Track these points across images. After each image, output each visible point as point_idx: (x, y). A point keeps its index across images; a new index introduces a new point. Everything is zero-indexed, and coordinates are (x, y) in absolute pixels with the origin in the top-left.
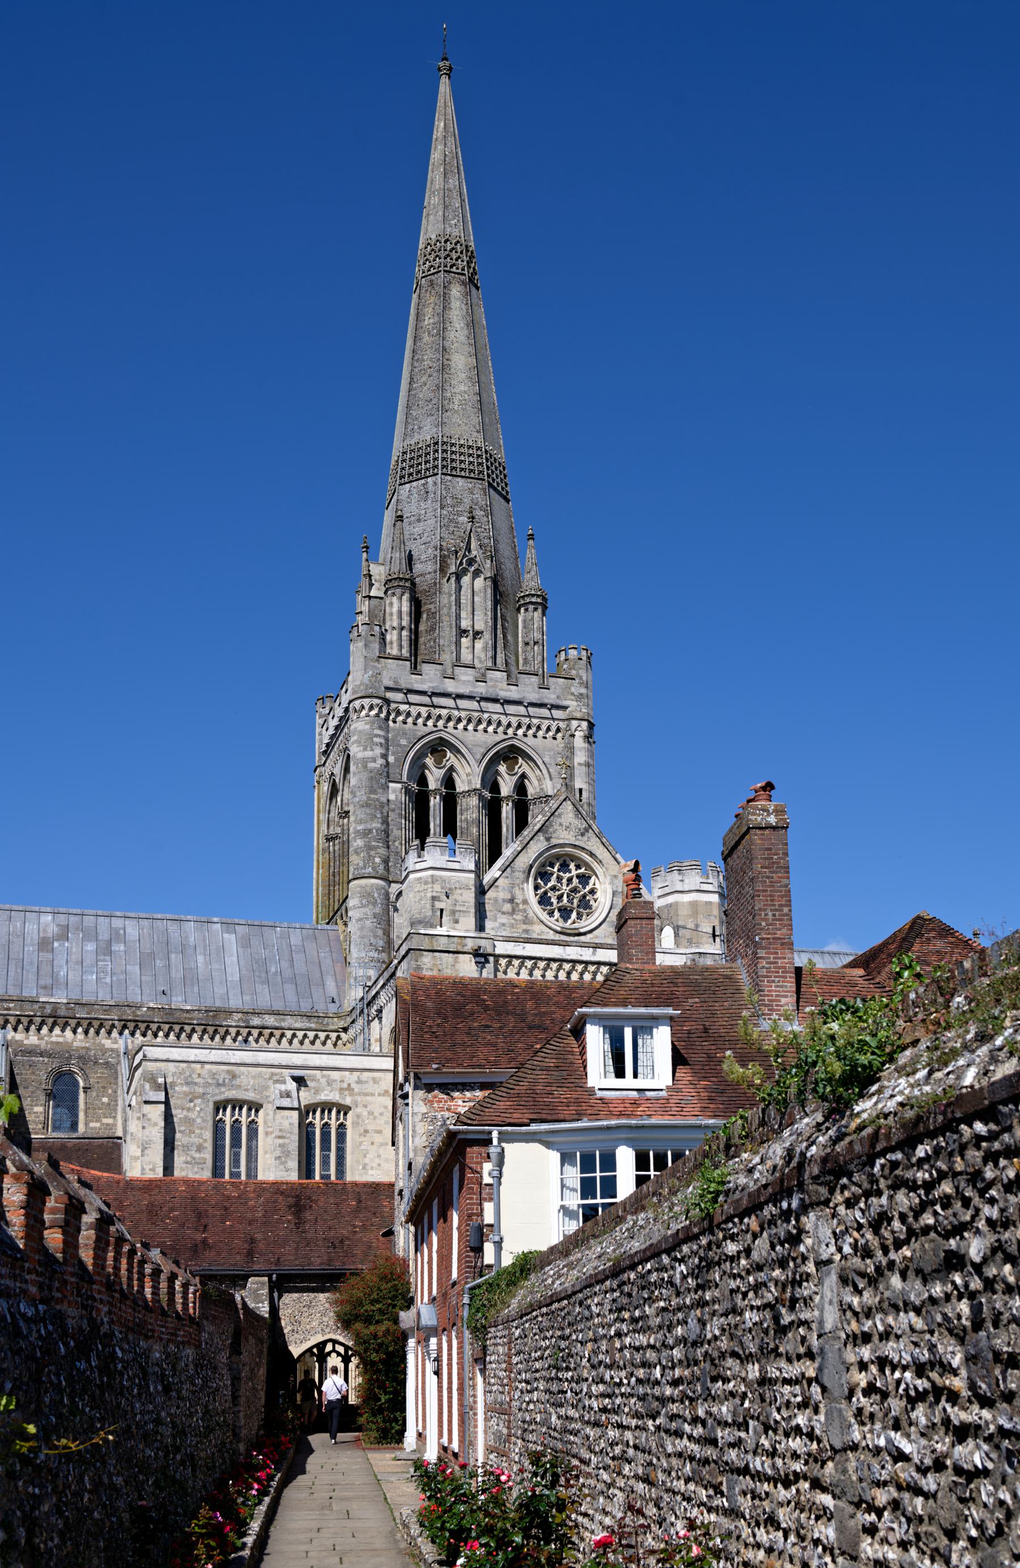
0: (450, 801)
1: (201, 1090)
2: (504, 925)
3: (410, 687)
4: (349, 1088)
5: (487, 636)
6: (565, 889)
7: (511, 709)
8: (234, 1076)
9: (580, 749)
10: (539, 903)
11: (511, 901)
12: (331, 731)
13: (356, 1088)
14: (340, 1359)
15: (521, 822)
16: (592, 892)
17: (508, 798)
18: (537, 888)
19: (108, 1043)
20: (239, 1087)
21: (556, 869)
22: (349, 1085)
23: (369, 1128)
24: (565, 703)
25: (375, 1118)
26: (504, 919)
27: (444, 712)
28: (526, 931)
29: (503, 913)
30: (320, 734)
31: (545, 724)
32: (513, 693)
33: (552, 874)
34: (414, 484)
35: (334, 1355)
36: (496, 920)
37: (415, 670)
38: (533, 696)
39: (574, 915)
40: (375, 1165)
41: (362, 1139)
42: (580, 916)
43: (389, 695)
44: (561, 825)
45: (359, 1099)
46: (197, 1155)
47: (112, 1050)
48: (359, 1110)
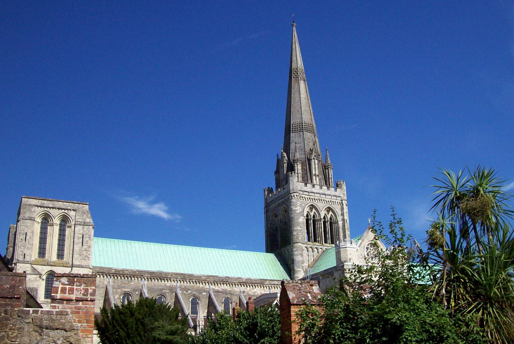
3: (304, 190)
24: (341, 196)
33: (368, 248)
34: (296, 133)
43: (299, 192)
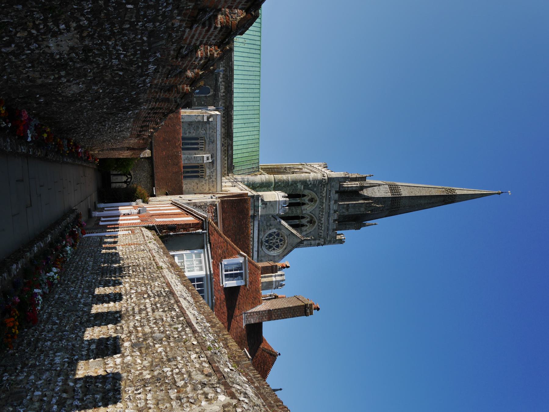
1: (208, 132)
2: (263, 223)
4: (211, 178)
5: (347, 213)
6: (274, 241)
7: (327, 222)
8: (212, 143)
9: (315, 242)
10: (270, 234)
12: (317, 168)
13: (211, 180)
14: (126, 180)
16: (274, 249)
17: (300, 221)
18: (275, 232)
19: (220, 103)
20: (209, 144)
21: (280, 238)
22: (212, 178)
23: (199, 185)
24: (329, 237)
25: (202, 187)
26: (265, 223)
27: (324, 201)
28: (261, 230)
29: (266, 223)
30: (316, 164)
31: (322, 232)
32: (331, 221)
35: (127, 178)
36: (264, 220)
38: (330, 227)
39: (267, 244)
40: (187, 187)
41: (195, 183)
42: (266, 246)
44: (294, 238)
46: (187, 132)
47: (218, 105)
48: (204, 181)
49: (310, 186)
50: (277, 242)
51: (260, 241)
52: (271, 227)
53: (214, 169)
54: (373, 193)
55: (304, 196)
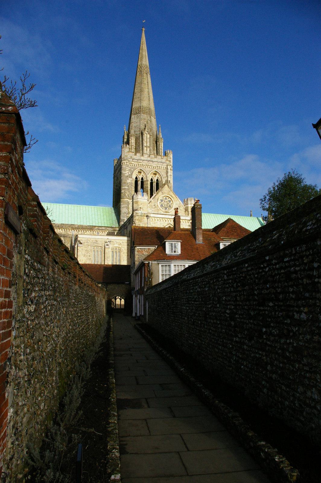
0: (142, 183)
2: (153, 210)
6: (166, 203)
11: (155, 205)
13: (122, 244)
15: (157, 189)
18: (160, 203)
26: (153, 209)
27: (141, 164)
28: (158, 212)
35: (118, 299)
37: (136, 155)
38: (160, 161)
39: (168, 209)
42: (169, 209)
45: (123, 246)
49: (130, 173)
50: (167, 202)
51: (165, 213)
52: (156, 205)
53: (114, 241)
54: (138, 127)
55: (136, 178)
